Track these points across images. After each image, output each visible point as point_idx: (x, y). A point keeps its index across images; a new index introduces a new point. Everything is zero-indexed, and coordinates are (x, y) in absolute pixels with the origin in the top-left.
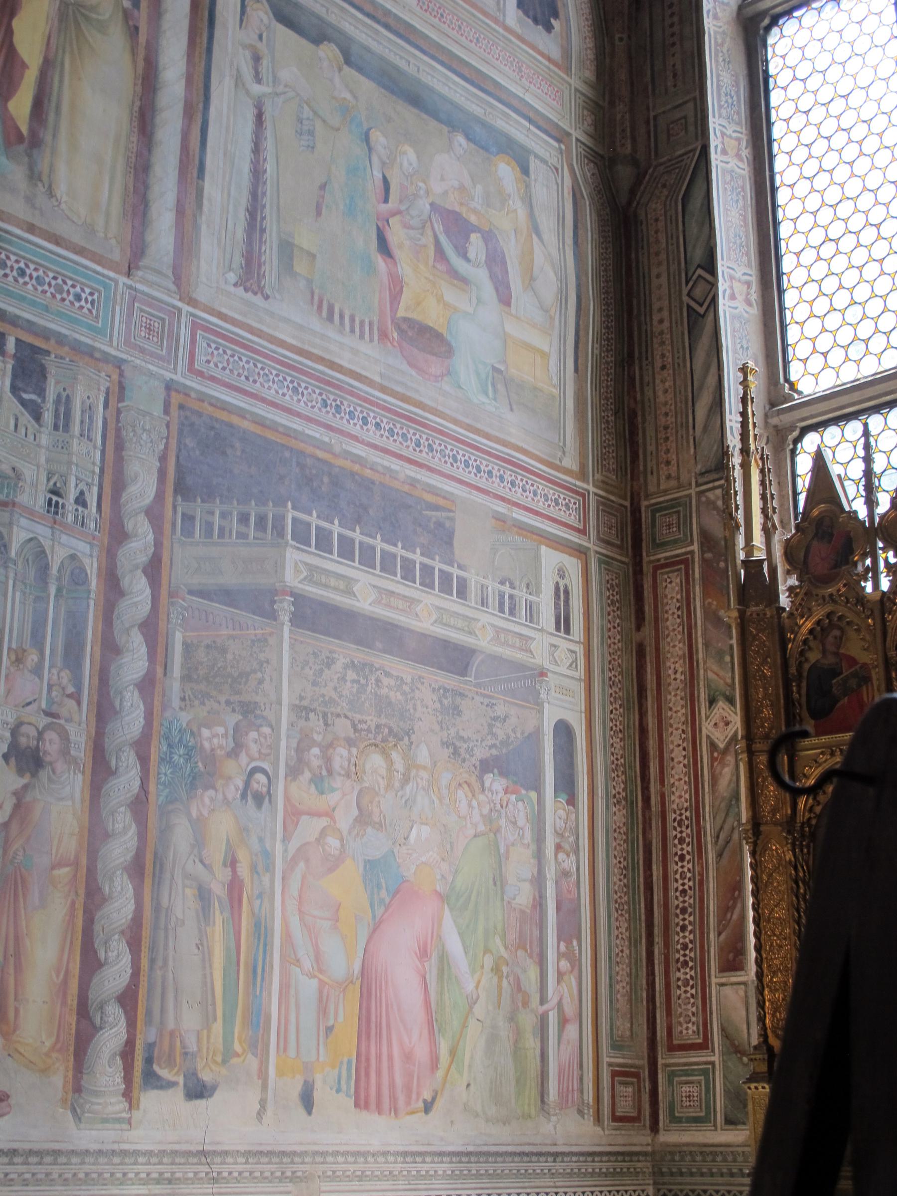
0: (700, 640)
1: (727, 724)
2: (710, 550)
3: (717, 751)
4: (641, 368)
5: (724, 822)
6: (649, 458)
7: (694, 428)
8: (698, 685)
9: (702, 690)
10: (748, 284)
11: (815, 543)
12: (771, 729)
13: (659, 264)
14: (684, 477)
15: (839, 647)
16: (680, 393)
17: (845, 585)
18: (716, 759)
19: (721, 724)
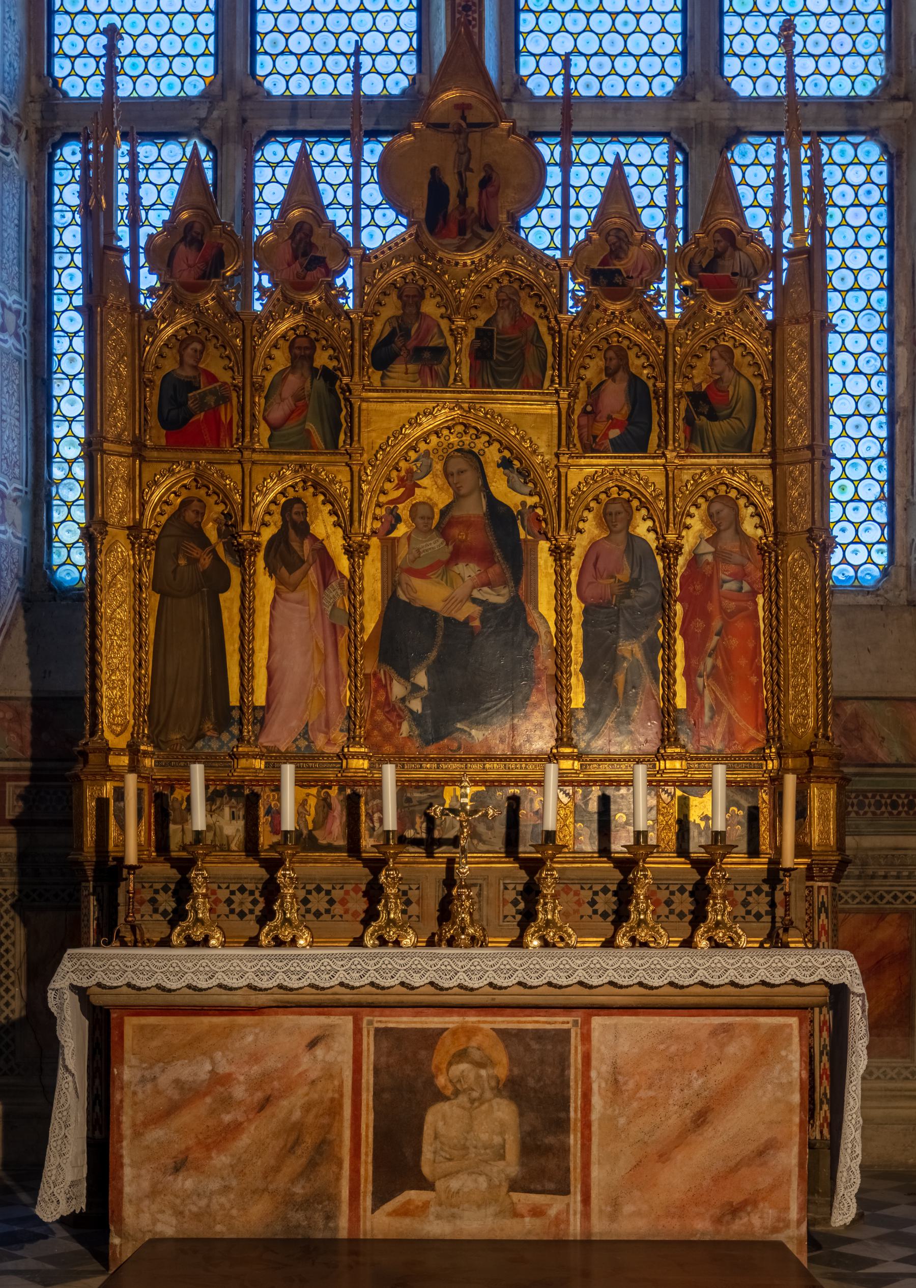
11: (182, 247)
12: (123, 430)
15: (198, 361)
17: (213, 299)
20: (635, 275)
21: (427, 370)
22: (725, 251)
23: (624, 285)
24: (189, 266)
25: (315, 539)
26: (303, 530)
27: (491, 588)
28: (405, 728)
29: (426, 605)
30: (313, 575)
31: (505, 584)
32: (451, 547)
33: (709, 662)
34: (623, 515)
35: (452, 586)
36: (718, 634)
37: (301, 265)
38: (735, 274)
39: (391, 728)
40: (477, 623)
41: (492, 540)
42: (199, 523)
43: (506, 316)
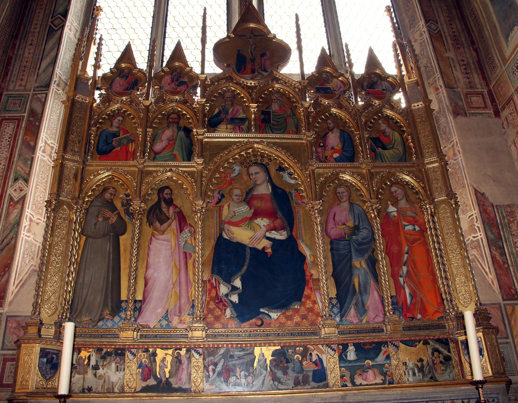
0: (17, 153)
1: (21, 190)
2: (32, 117)
3: (13, 201)
4: (20, 43)
5: (9, 234)
6: (13, 76)
7: (39, 69)
8: (11, 171)
9: (12, 174)
10: (77, 31)
11: (118, 78)
13: (41, 9)
14: (28, 86)
16: (36, 55)
18: (12, 205)
19: (18, 190)
20: (337, 90)
21: (237, 127)
22: (377, 81)
23: (332, 93)
24: (120, 86)
25: (176, 207)
26: (170, 202)
27: (277, 232)
28: (228, 312)
29: (239, 241)
30: (174, 225)
31: (283, 228)
32: (253, 210)
33: (405, 269)
34: (346, 193)
35: (254, 230)
36: (407, 253)
37: (175, 84)
38: (383, 90)
39: (220, 313)
40: (269, 250)
41: (276, 206)
42: (112, 200)
43: (276, 106)
